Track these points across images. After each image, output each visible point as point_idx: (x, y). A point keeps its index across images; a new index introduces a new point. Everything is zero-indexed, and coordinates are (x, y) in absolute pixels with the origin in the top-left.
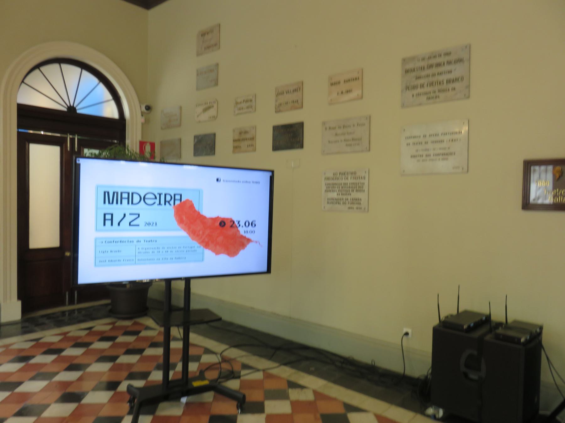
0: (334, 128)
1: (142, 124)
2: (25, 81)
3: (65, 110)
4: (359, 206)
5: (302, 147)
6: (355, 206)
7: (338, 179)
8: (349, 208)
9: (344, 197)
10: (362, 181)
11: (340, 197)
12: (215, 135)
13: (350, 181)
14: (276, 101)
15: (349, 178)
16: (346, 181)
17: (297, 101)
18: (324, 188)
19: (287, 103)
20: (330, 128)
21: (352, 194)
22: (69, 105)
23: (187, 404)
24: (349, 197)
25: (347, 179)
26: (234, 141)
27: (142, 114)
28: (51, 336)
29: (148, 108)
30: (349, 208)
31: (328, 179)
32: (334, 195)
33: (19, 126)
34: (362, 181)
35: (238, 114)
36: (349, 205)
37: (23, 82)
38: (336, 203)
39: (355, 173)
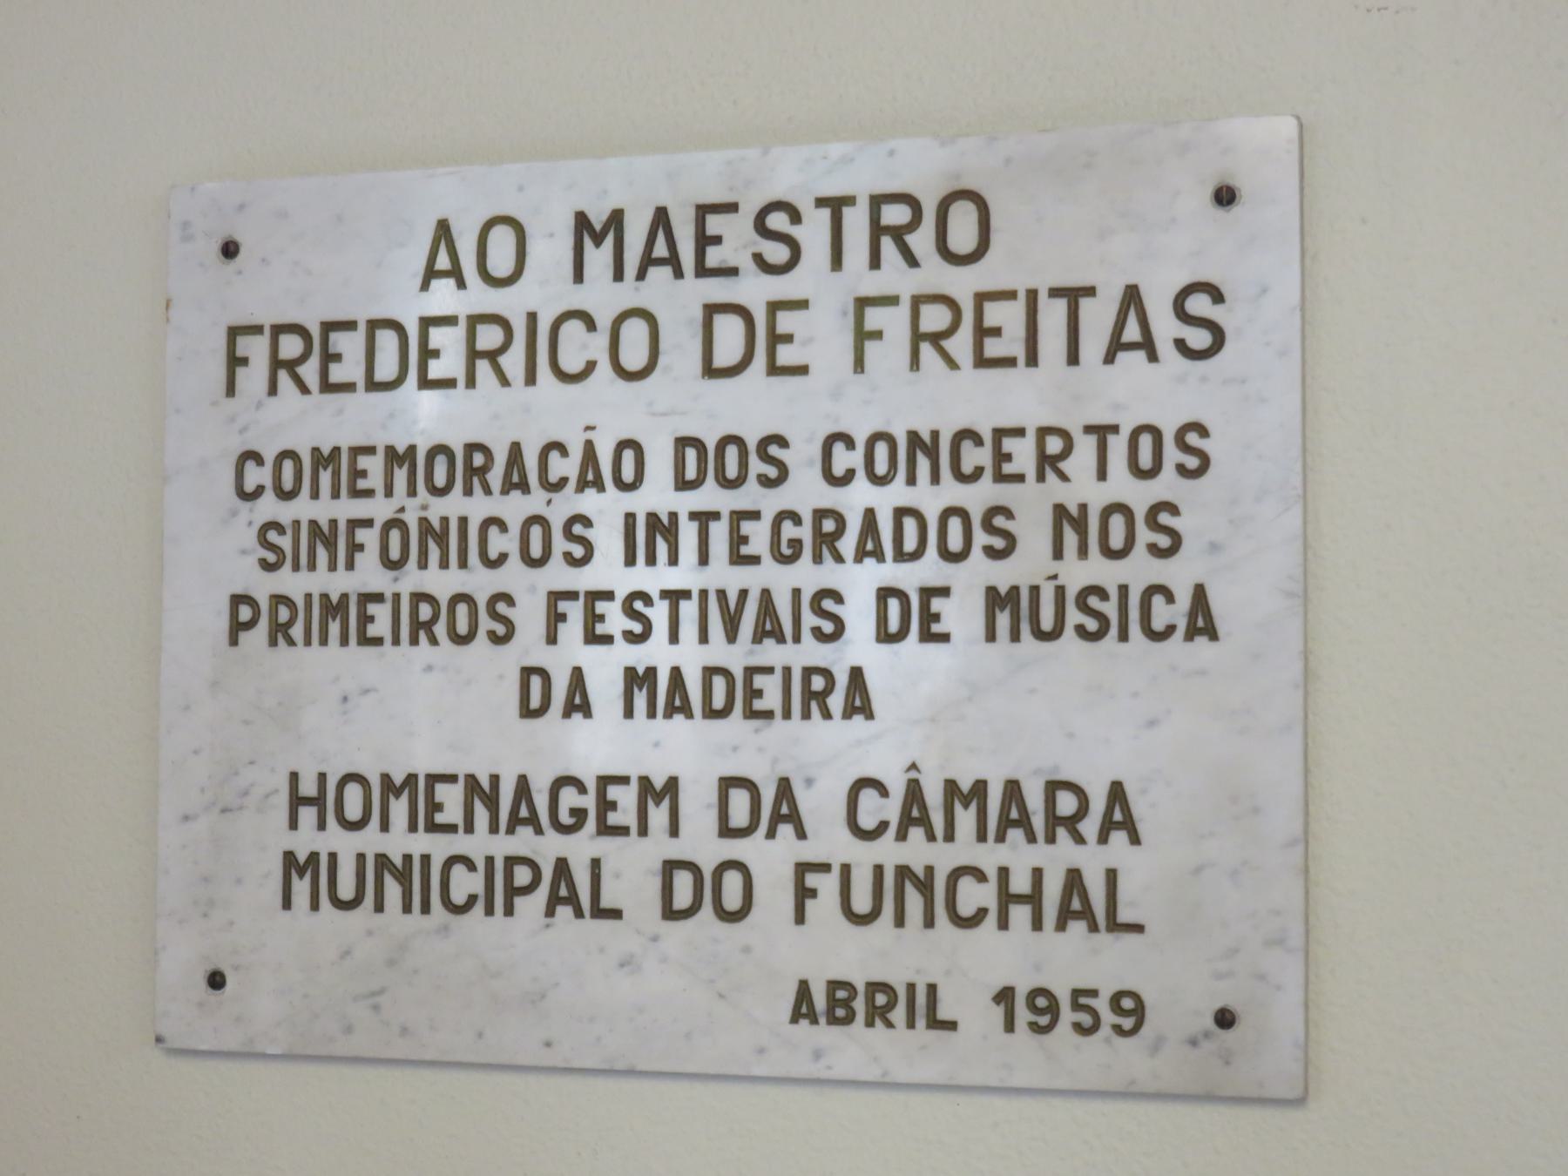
4: (1069, 959)
6: (975, 964)
7: (540, 349)
8: (831, 1005)
9: (689, 751)
10: (1149, 392)
11: (603, 743)
13: (840, 391)
15: (820, 336)
16: (749, 406)
21: (897, 671)
24: (824, 754)
25: (770, 347)
30: (831, 1005)
31: (304, 353)
32: (432, 711)
34: (1149, 392)
36: (842, 952)
38: (505, 888)
39: (957, 217)
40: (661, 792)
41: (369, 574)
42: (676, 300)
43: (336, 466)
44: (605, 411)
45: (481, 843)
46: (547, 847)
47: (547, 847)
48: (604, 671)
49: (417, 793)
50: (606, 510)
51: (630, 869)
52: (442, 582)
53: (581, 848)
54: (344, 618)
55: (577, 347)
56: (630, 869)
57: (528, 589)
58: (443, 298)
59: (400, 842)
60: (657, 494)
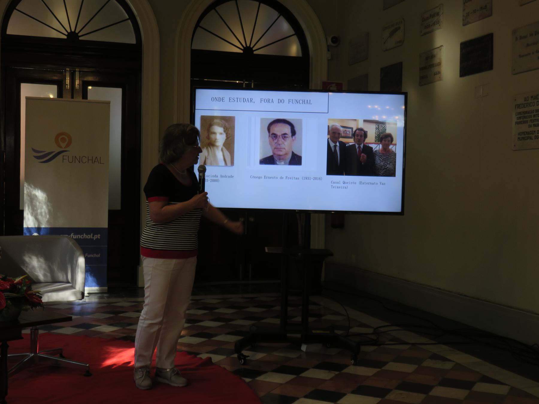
0: (525, 37)
1: (328, 60)
2: (201, 24)
3: (242, 52)
5: (490, 67)
11: (532, 129)
12: (401, 64)
14: (464, 10)
17: (486, 6)
18: (515, 120)
19: (475, 11)
20: (521, 38)
22: (245, 46)
23: (307, 353)
26: (422, 69)
27: (329, 48)
28: (211, 300)
29: (335, 40)
31: (518, 106)
32: (524, 128)
33: (192, 76)
35: (425, 34)
37: (197, 25)
40: (535, 131)
41: (522, 120)
42: (535, 101)
43: (520, 113)
44: (533, 108)
45: (527, 136)
46: (529, 135)
47: (529, 135)
48: (532, 124)
49: (523, 133)
50: (532, 114)
51: (533, 136)
52: (525, 120)
53: (531, 135)
54: (520, 123)
55: (531, 104)
56: (533, 136)
57: (529, 119)
58: (526, 102)
59: (523, 136)
60: (535, 113)
